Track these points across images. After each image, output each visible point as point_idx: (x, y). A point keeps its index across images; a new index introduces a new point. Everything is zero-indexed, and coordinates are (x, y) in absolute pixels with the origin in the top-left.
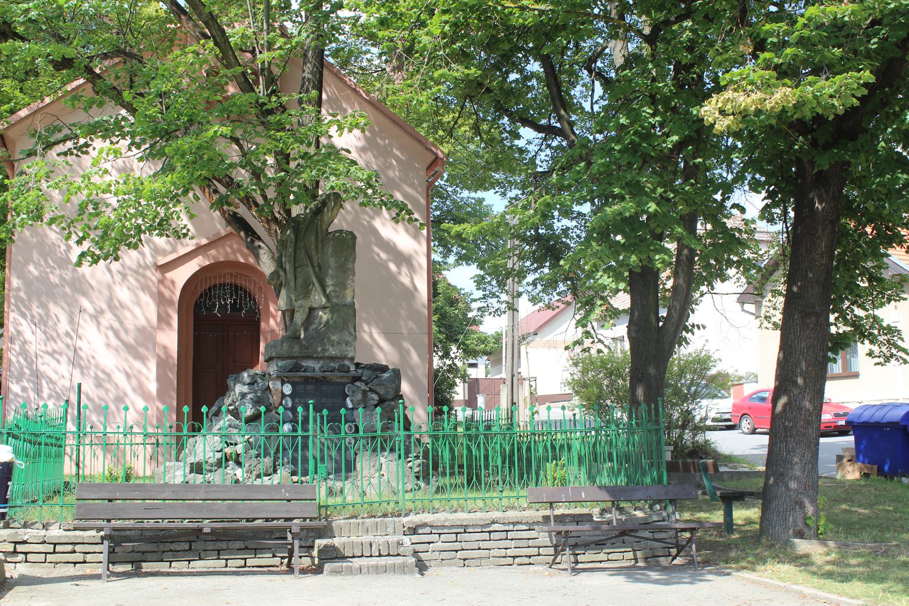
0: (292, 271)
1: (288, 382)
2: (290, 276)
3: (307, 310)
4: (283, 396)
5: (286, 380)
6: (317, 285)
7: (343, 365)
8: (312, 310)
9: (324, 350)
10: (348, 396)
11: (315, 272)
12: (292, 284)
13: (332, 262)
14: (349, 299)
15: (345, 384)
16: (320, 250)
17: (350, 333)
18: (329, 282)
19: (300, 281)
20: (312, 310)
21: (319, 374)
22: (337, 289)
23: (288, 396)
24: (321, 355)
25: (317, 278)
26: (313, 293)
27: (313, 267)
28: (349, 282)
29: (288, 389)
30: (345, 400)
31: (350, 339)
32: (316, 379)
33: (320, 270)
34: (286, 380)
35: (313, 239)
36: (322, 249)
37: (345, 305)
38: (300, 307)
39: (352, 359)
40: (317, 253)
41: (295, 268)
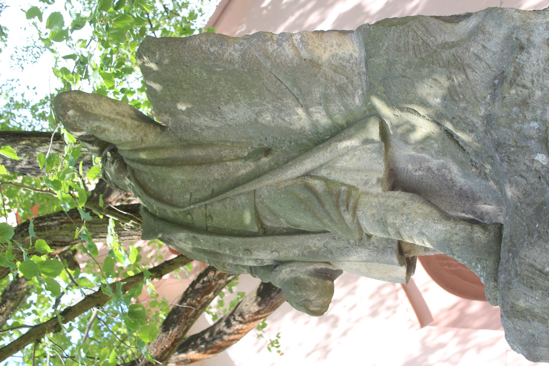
0: (273, 242)
2: (290, 248)
3: (399, 198)
6: (308, 164)
8: (395, 181)
11: (272, 169)
12: (315, 242)
13: (237, 113)
14: (352, 49)
16: (211, 152)
17: (478, 30)
18: (300, 119)
19: (302, 220)
20: (395, 181)
22: (317, 92)
25: (290, 159)
26: (334, 176)
27: (256, 175)
28: (288, 51)
31: (497, 35)
33: (267, 152)
35: (178, 176)
36: (211, 144)
37: (369, 57)
38: (383, 223)
40: (220, 161)
41: (266, 232)
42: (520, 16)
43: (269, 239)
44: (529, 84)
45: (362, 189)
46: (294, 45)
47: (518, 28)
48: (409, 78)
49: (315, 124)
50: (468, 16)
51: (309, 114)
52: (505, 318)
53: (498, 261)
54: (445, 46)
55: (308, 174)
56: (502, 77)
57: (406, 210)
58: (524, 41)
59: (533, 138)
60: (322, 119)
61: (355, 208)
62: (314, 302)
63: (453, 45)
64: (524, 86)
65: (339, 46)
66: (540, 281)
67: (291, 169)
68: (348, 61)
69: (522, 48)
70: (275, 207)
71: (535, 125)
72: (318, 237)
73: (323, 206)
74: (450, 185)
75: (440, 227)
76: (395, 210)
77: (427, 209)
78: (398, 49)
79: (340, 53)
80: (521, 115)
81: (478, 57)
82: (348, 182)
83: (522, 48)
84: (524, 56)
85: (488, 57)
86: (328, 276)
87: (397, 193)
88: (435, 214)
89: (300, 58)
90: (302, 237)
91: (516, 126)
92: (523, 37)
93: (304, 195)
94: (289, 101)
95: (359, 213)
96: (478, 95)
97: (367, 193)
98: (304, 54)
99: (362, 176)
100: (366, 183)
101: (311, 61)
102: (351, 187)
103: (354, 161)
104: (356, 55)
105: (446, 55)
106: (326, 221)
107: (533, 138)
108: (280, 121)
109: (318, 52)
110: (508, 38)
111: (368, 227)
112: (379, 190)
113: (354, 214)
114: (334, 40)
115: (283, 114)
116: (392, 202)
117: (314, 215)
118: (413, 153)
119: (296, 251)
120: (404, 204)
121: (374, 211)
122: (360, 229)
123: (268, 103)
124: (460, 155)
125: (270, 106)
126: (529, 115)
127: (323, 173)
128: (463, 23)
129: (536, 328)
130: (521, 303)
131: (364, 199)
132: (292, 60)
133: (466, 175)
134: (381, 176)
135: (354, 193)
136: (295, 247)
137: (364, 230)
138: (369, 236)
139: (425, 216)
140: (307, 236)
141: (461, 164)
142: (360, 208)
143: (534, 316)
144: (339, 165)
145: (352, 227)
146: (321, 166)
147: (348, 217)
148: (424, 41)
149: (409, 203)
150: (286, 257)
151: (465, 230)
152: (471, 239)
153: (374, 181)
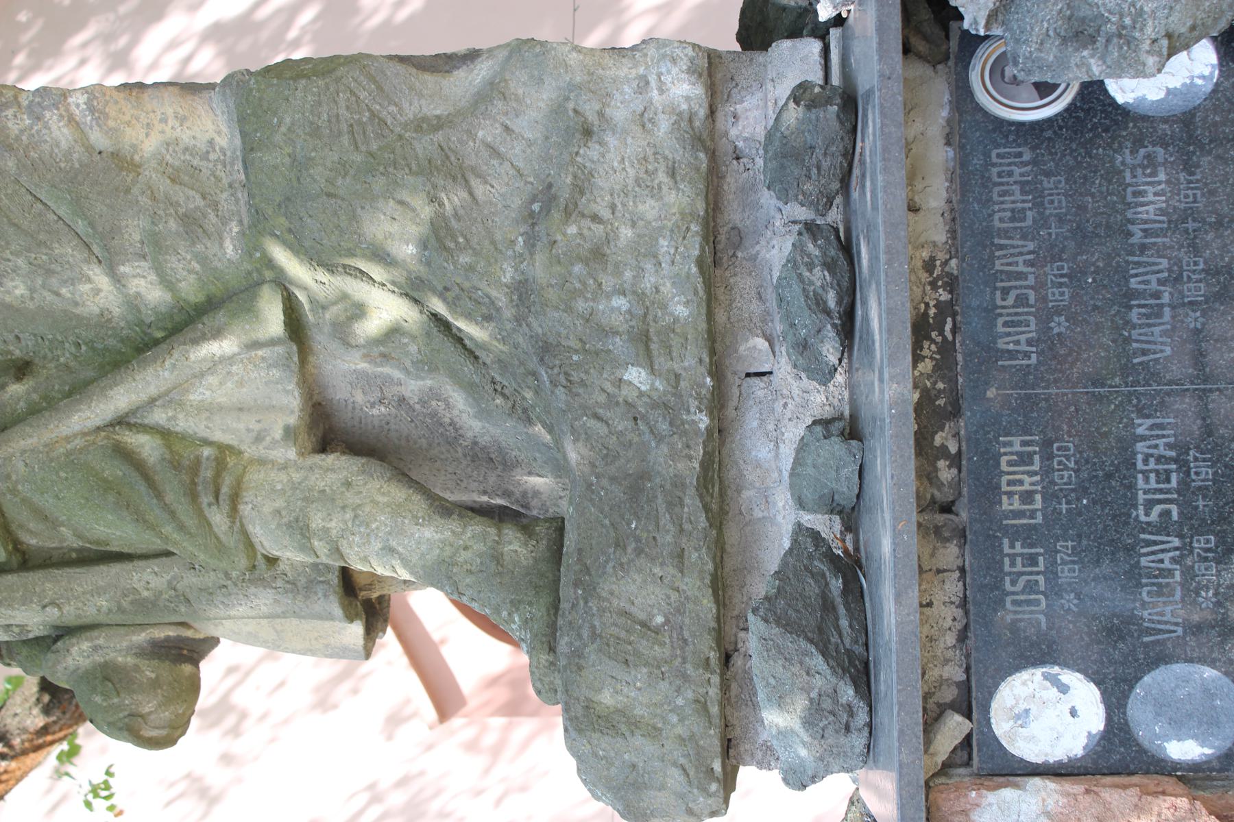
0: (46, 583)
1: (970, 700)
2: (88, 595)
5: (955, 727)
7: (786, 155)
8: (327, 431)
9: (645, 340)
10: (1093, 92)
11: (34, 412)
12: (146, 579)
14: (212, 128)
15: (972, 129)
17: (493, 90)
18: (98, 293)
19: (115, 530)
20: (327, 431)
21: (889, 386)
22: (134, 230)
23: (1115, 702)
24: (691, 362)
25: (78, 390)
26: (184, 424)
28: (59, 132)
30: (1119, 114)
31: (534, 105)
32: (931, 412)
34: (955, 727)
37: (249, 147)
38: (300, 530)
39: (713, 71)
42: (582, 62)
44: (606, 214)
45: (250, 451)
46: (71, 119)
47: (579, 87)
48: (343, 199)
49: (133, 304)
50: (472, 56)
51: (117, 279)
52: (573, 734)
53: (555, 606)
54: (424, 125)
55: (122, 421)
56: (546, 196)
57: (351, 498)
58: (592, 117)
59: (617, 333)
60: (149, 290)
61: (235, 499)
62: (153, 717)
63: (438, 124)
64: (596, 218)
65: (182, 120)
66: (643, 646)
67: (80, 410)
68: (205, 157)
69: (588, 133)
70: (46, 502)
71: (620, 302)
72: (154, 565)
73: (159, 495)
74: (452, 435)
75: (428, 533)
76: (326, 498)
77: (398, 493)
78: (315, 132)
79: (185, 137)
80: (591, 281)
81: (494, 151)
82: (218, 436)
83: (588, 133)
84: (593, 151)
85: (516, 151)
86: (186, 653)
87: (330, 459)
88: (418, 503)
89: (89, 148)
90: (115, 569)
91: (581, 305)
92: (590, 109)
93: (114, 470)
94: (68, 250)
95: (245, 509)
96: (498, 237)
97: (262, 462)
98: (97, 138)
99: (250, 422)
100: (259, 439)
101: (115, 155)
102: (223, 449)
103: (229, 388)
104: (222, 142)
106: (168, 529)
107: (617, 333)
108: (50, 297)
109: (132, 135)
110: (558, 110)
111: (267, 540)
112: (292, 454)
113: (234, 511)
114: (170, 105)
115: (54, 281)
116: (319, 481)
117: (140, 519)
118: (363, 365)
119: (103, 603)
120: (348, 484)
121: (280, 503)
122: (250, 545)
123: (16, 254)
124: (468, 368)
125: (20, 262)
126: (608, 282)
127: (159, 417)
128: (460, 73)
129: (639, 749)
130: (607, 698)
131: (255, 476)
132: (68, 153)
133: (483, 414)
134: (292, 420)
135: (231, 461)
136: (99, 591)
137: (258, 547)
138: (272, 561)
139: (396, 510)
140: (128, 566)
141: (470, 389)
142: (248, 496)
143: (635, 725)
144: (194, 397)
145: (230, 541)
146: (152, 401)
147: (218, 519)
148: (373, 115)
149: (359, 480)
150: (79, 616)
151: (484, 537)
152: (497, 558)
153: (278, 433)
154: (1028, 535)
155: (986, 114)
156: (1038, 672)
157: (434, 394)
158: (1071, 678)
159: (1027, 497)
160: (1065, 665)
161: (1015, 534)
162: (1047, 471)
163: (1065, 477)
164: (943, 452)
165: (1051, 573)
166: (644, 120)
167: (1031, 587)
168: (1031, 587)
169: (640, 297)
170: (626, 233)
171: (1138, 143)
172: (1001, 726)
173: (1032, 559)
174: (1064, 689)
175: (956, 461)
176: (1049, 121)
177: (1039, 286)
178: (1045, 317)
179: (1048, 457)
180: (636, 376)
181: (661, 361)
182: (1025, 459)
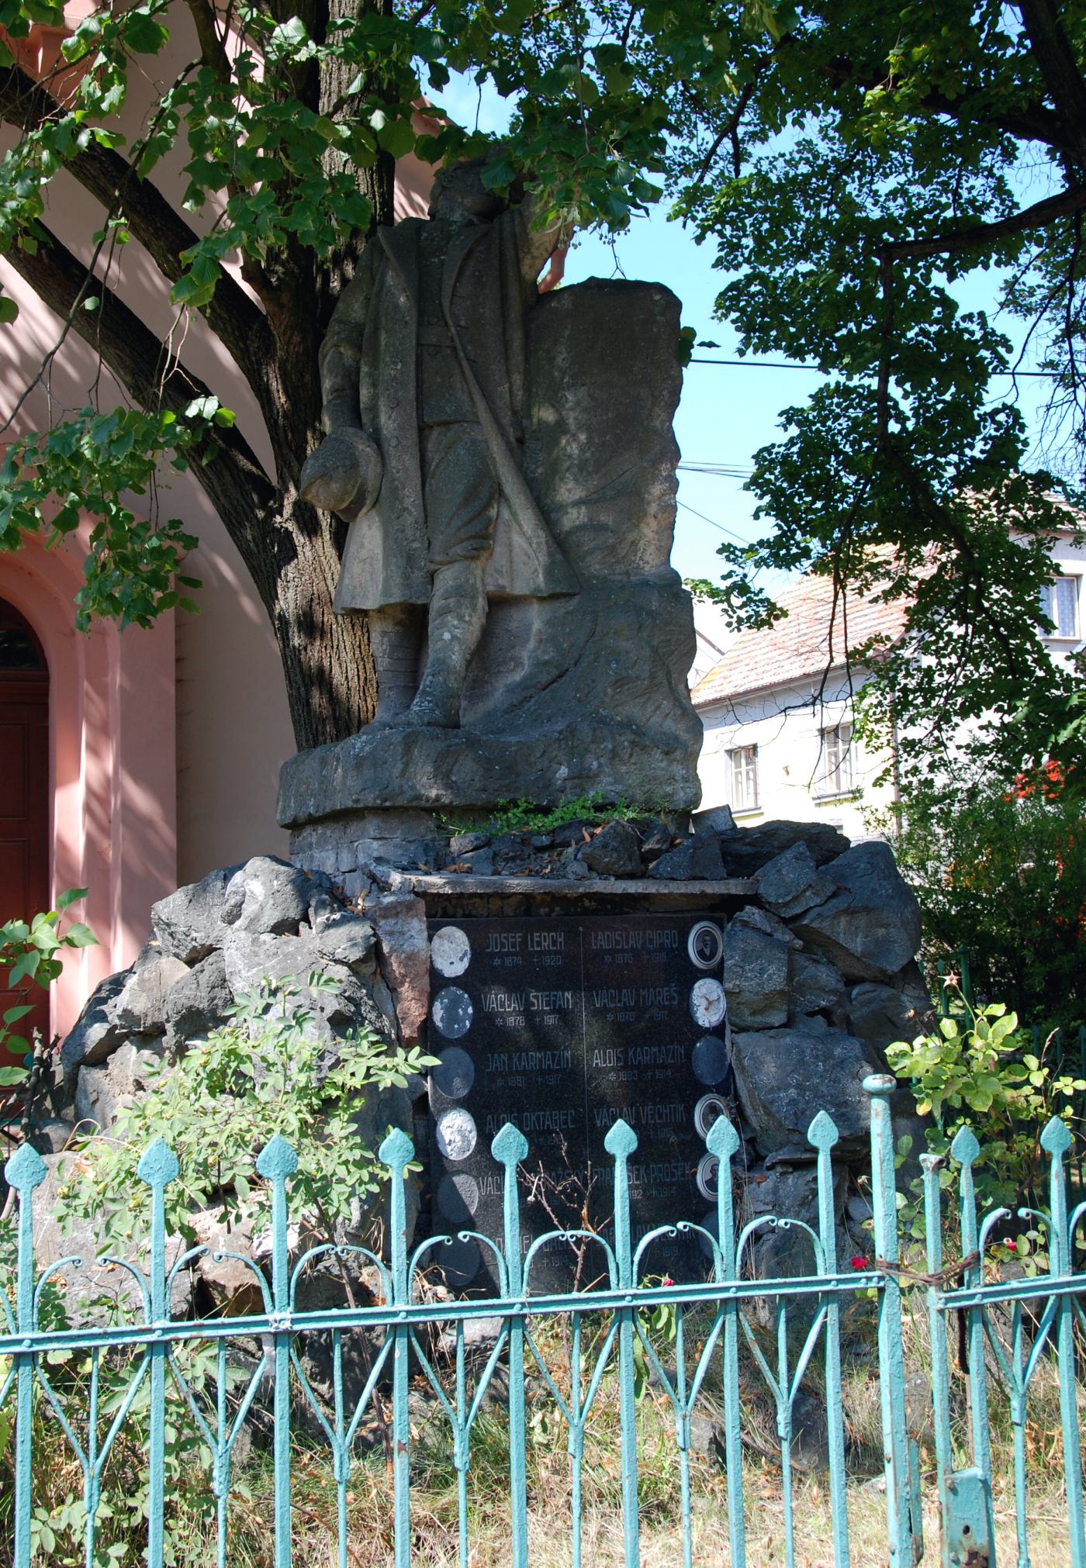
4: (437, 983)
18: (568, 491)
23: (456, 981)
28: (657, 490)
29: (452, 952)
41: (423, 430)
43: (413, 436)
44: (633, 760)
56: (639, 732)
58: (673, 756)
64: (631, 755)
68: (641, 559)
71: (595, 764)
92: (678, 754)
96: (620, 709)
100: (498, 572)
104: (647, 568)
105: (661, 676)
110: (676, 738)
115: (575, 470)
123: (593, 454)
125: (588, 455)
126: (602, 760)
133: (511, 689)
140: (419, 487)
153: (501, 582)
154: (524, 942)
155: (691, 928)
156: (468, 948)
157: (519, 664)
158: (466, 961)
159: (539, 944)
160: (471, 960)
161: (524, 938)
162: (549, 952)
163: (549, 961)
164: (552, 911)
165: (508, 954)
166: (672, 779)
167: (503, 945)
168: (503, 945)
169: (597, 776)
170: (623, 769)
171: (680, 993)
172: (446, 930)
173: (514, 946)
174: (461, 959)
175: (549, 915)
176: (688, 955)
177: (623, 951)
178: (612, 952)
179: (555, 953)
180: (563, 771)
181: (569, 784)
182: (554, 943)
